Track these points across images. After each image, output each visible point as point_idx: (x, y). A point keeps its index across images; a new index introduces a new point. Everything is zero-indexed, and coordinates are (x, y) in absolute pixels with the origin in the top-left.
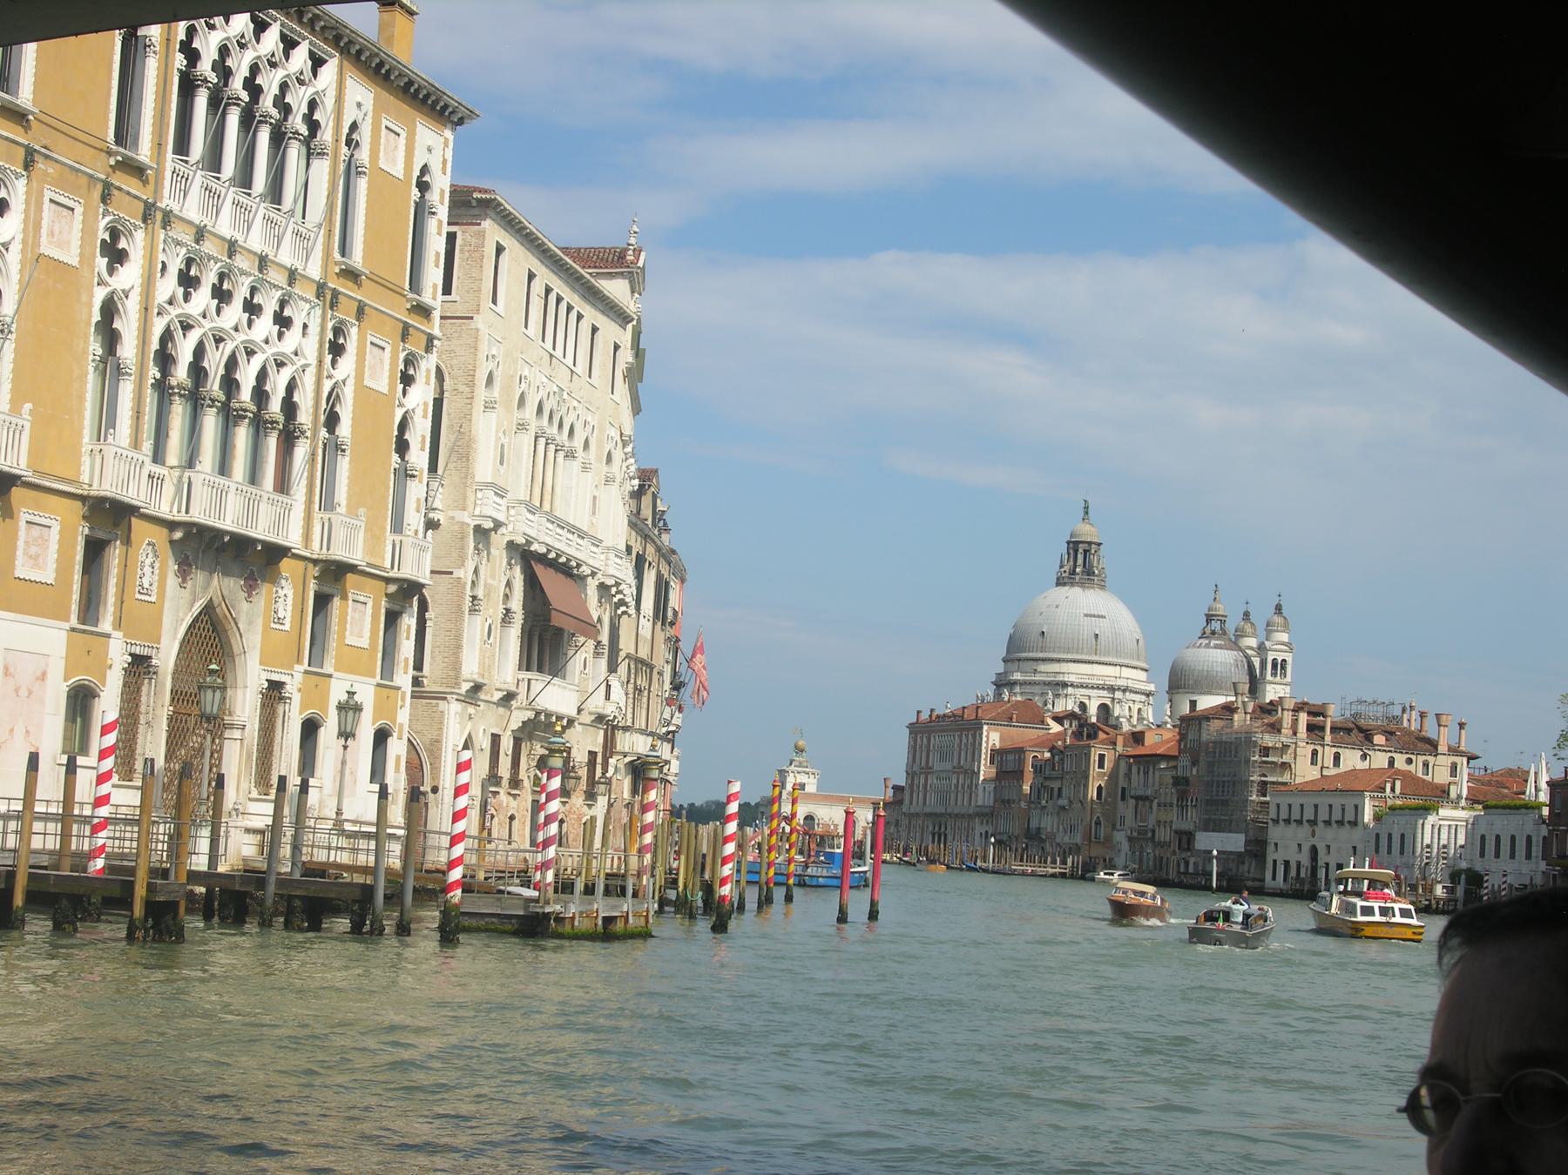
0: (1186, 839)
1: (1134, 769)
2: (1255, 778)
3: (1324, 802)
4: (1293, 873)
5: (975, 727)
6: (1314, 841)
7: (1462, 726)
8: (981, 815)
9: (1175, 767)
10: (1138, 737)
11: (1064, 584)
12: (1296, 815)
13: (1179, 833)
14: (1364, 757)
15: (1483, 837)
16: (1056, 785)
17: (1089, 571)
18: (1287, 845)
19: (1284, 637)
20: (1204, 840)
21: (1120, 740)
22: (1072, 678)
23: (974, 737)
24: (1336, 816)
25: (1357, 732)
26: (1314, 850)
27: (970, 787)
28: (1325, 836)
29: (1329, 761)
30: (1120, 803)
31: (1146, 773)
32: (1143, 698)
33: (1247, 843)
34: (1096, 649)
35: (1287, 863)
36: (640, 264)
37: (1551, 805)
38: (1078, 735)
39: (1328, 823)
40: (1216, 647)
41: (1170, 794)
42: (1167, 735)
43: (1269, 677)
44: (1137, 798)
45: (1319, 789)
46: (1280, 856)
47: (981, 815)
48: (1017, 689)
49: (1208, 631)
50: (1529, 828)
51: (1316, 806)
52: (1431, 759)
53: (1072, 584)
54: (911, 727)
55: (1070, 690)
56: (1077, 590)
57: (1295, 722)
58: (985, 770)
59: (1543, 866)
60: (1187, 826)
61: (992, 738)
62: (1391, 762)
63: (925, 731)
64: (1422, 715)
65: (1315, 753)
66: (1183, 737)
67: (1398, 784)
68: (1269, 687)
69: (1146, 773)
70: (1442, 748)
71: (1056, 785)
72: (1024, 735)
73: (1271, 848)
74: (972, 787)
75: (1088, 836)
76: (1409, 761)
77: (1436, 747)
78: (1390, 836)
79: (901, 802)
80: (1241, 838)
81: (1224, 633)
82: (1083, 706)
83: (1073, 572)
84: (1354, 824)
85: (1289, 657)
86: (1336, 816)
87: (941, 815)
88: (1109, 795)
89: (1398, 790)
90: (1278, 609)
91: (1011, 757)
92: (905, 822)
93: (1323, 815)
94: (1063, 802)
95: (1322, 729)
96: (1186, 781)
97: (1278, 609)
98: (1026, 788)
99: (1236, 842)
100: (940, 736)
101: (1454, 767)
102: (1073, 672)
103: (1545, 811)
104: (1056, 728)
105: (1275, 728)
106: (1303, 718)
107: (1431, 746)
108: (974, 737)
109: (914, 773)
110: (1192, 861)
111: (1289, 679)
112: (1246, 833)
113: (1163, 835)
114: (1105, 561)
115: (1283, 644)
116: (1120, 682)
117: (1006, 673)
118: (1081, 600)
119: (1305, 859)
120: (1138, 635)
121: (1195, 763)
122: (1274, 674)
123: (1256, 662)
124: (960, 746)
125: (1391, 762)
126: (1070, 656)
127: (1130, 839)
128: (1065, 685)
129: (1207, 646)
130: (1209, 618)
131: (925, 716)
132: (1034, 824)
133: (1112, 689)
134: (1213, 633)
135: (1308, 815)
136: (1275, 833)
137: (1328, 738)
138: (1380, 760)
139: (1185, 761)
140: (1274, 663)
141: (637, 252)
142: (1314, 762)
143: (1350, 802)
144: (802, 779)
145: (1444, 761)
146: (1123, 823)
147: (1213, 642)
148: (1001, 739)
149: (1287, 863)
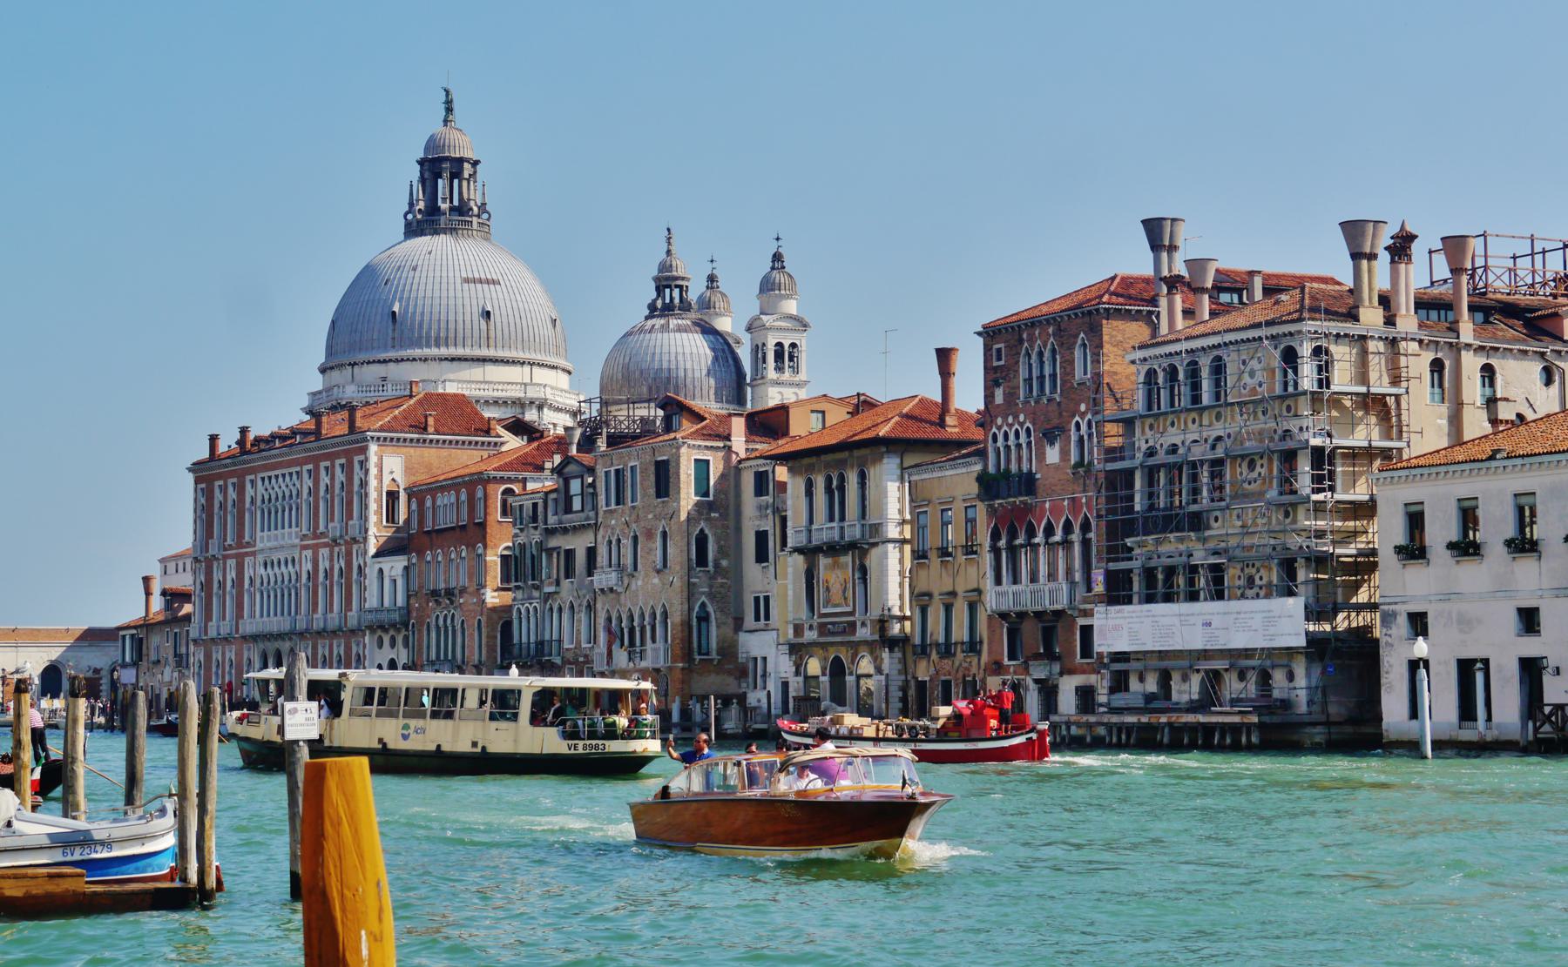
5: (355, 446)
11: (422, 233)
16: (579, 544)
17: (462, 209)
23: (348, 469)
27: (345, 573)
34: (485, 339)
40: (679, 329)
43: (771, 374)
44: (810, 552)
49: (659, 304)
53: (436, 232)
54: (197, 467)
56: (443, 240)
58: (377, 532)
61: (389, 467)
71: (579, 544)
74: (350, 577)
87: (280, 636)
88: (722, 552)
91: (444, 499)
92: (197, 655)
96: (1028, 483)
108: (348, 469)
114: (484, 188)
115: (791, 317)
116: (532, 393)
117: (328, 390)
122: (779, 369)
124: (313, 492)
126: (443, 351)
131: (228, 442)
140: (779, 355)
147: (673, 322)
148: (408, 470)
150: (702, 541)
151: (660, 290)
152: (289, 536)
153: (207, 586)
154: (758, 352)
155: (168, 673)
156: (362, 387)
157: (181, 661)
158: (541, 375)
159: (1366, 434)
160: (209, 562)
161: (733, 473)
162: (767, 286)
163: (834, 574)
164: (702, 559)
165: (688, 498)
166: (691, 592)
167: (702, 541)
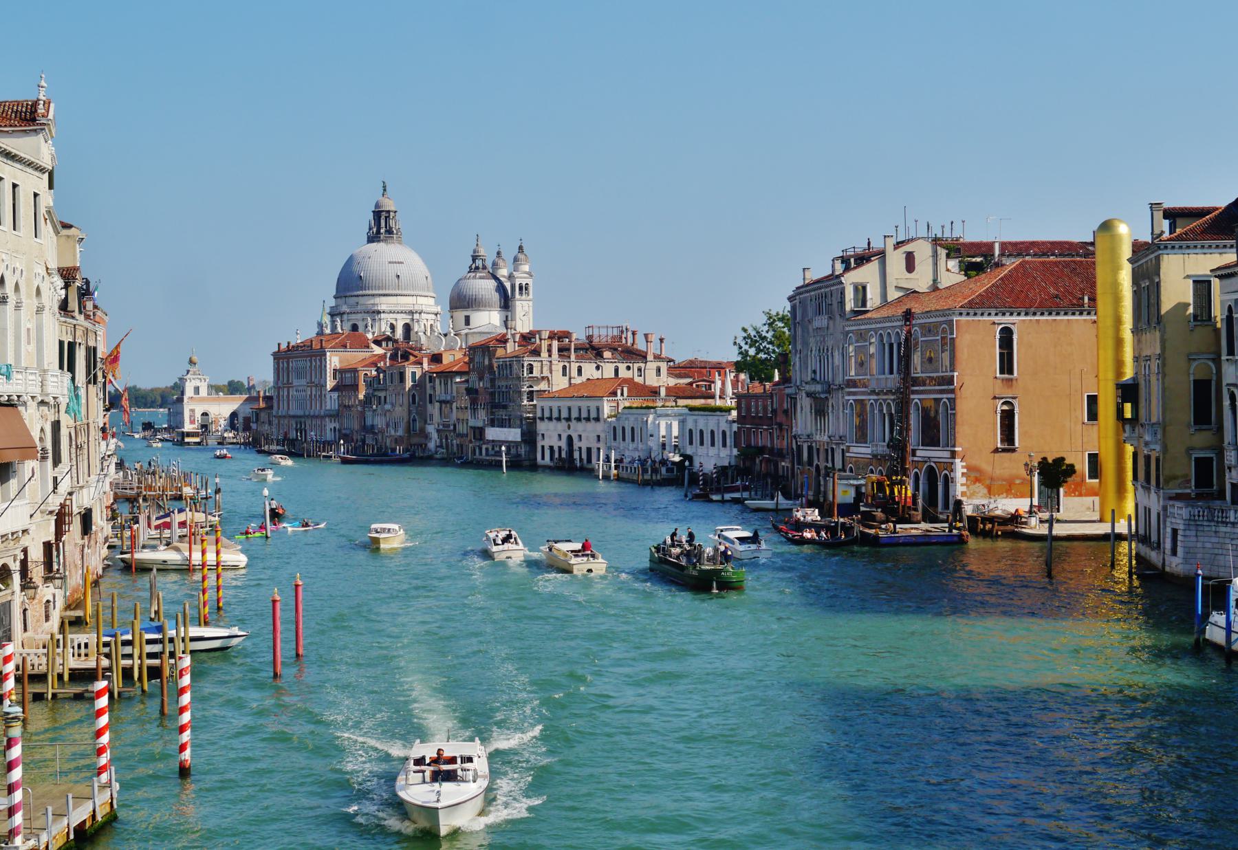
0: (479, 433)
1: (437, 381)
2: (525, 389)
3: (574, 404)
4: (557, 455)
6: (570, 432)
7: (661, 340)
8: (330, 416)
9: (467, 381)
10: (436, 358)
12: (555, 415)
13: (474, 428)
14: (598, 368)
15: (691, 431)
16: (382, 394)
17: (389, 231)
18: (551, 436)
19: (526, 268)
20: (492, 433)
21: (425, 361)
22: (382, 308)
24: (584, 415)
25: (593, 350)
26: (570, 438)
27: (320, 396)
28: (577, 428)
29: (574, 373)
30: (429, 406)
31: (446, 384)
32: (434, 317)
33: (523, 435)
34: (398, 286)
35: (551, 448)
36: (51, 116)
37: (738, 408)
38: (394, 357)
39: (579, 419)
41: (465, 401)
42: (459, 355)
43: (517, 296)
44: (441, 402)
45: (571, 393)
46: (547, 443)
47: (330, 416)
48: (345, 317)
50: (724, 426)
51: (569, 409)
52: (642, 365)
55: (383, 315)
56: (382, 244)
57: (550, 346)
58: (330, 383)
59: (735, 452)
60: (480, 424)
61: (334, 360)
62: (617, 370)
63: (284, 357)
64: (634, 333)
65: (564, 368)
66: (471, 360)
67: (625, 390)
68: (518, 303)
69: (446, 384)
70: (650, 357)
71: (382, 394)
72: (354, 357)
73: (539, 438)
75: (408, 430)
76: (628, 368)
77: (645, 357)
78: (624, 429)
79: (271, 407)
80: (519, 431)
81: (484, 267)
82: (393, 327)
83: (378, 232)
84: (597, 419)
85: (530, 281)
86: (584, 415)
89: (626, 393)
90: (521, 248)
91: (348, 375)
92: (275, 421)
93: (574, 414)
94: (388, 407)
95: (568, 350)
96: (476, 391)
97: (521, 248)
98: (361, 397)
99: (514, 434)
100: (295, 360)
101: (659, 370)
102: (384, 304)
103: (734, 413)
104: (378, 351)
105: (536, 352)
106: (555, 344)
107: (643, 357)
109: (279, 388)
110: (484, 447)
111: (531, 297)
112: (521, 426)
113: (462, 429)
114: (398, 223)
116: (417, 308)
118: (384, 252)
119: (563, 444)
120: (428, 274)
121: (481, 379)
122: (521, 294)
123: (508, 285)
125: (617, 370)
126: (381, 292)
127: (438, 431)
128: (379, 312)
129: (475, 277)
130: (474, 258)
131: (284, 346)
132: (369, 422)
133: (411, 313)
134: (477, 268)
135: (564, 414)
136: (542, 427)
137: (573, 357)
138: (608, 371)
139: (473, 377)
140: (521, 288)
141: (47, 104)
142: (564, 374)
143: (593, 404)
144: (198, 383)
145: (652, 366)
146: (431, 419)
149: (551, 448)
150: (414, 396)
151: (474, 261)
152: (303, 382)
153: (278, 396)
154: (513, 287)
155: (266, 427)
156: (350, 306)
157: (270, 423)
158: (421, 300)
159: (543, 386)
160: (279, 388)
161: (424, 375)
162: (516, 260)
163: (446, 409)
164: (414, 402)
165: (409, 383)
166: (410, 412)
167: (414, 396)
